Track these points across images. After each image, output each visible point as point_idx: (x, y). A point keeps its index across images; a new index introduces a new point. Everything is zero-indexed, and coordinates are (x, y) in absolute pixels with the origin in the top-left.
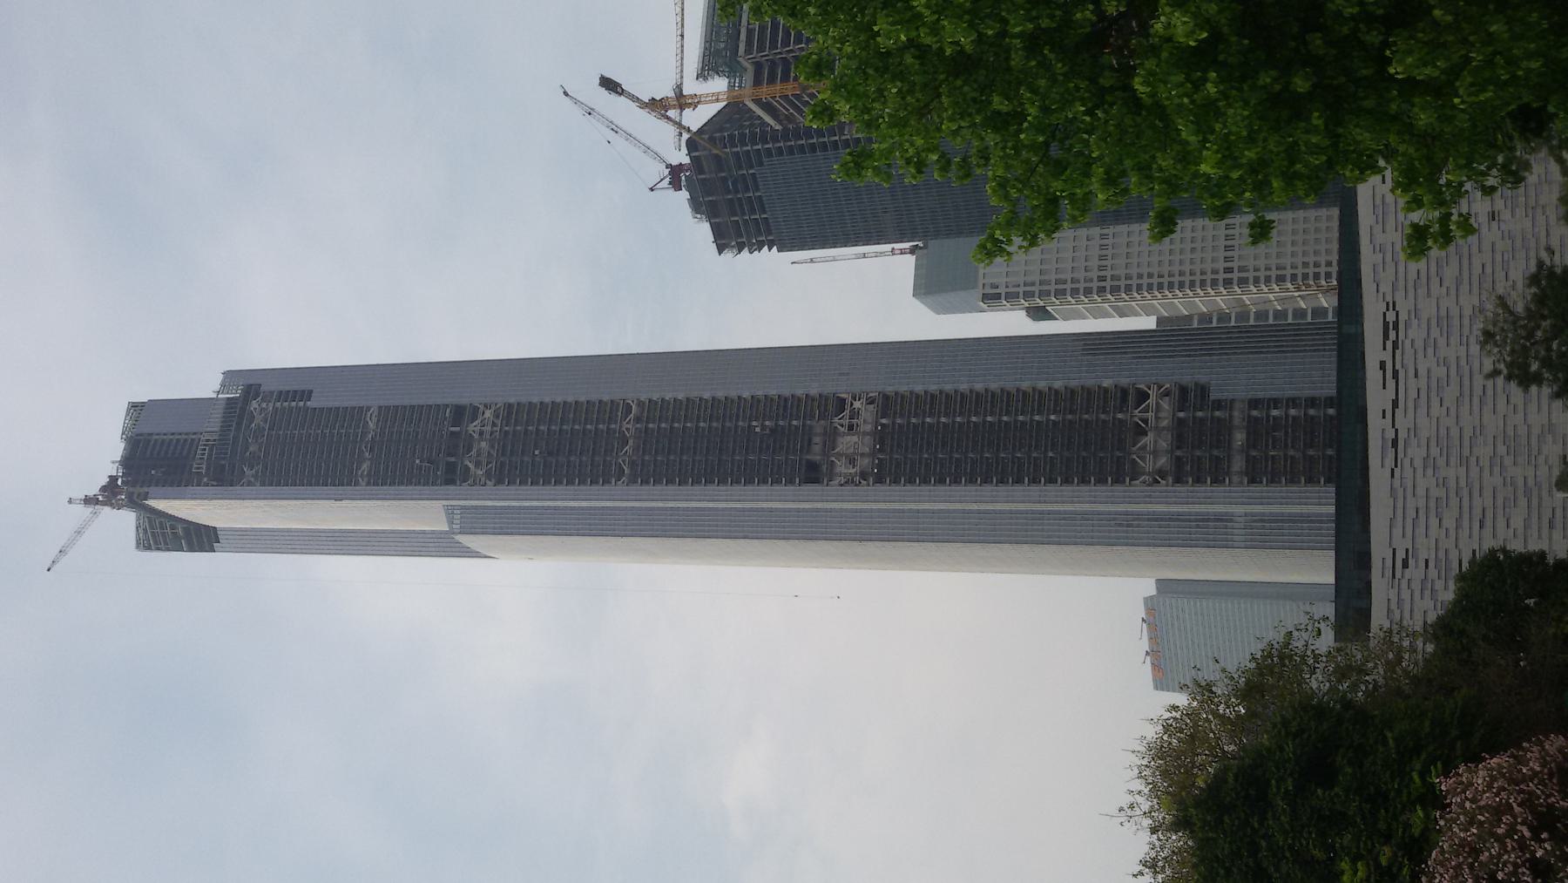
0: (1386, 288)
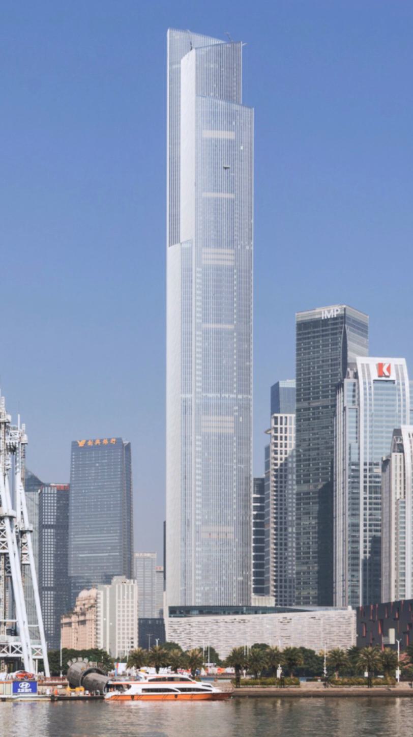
0: (253, 620)
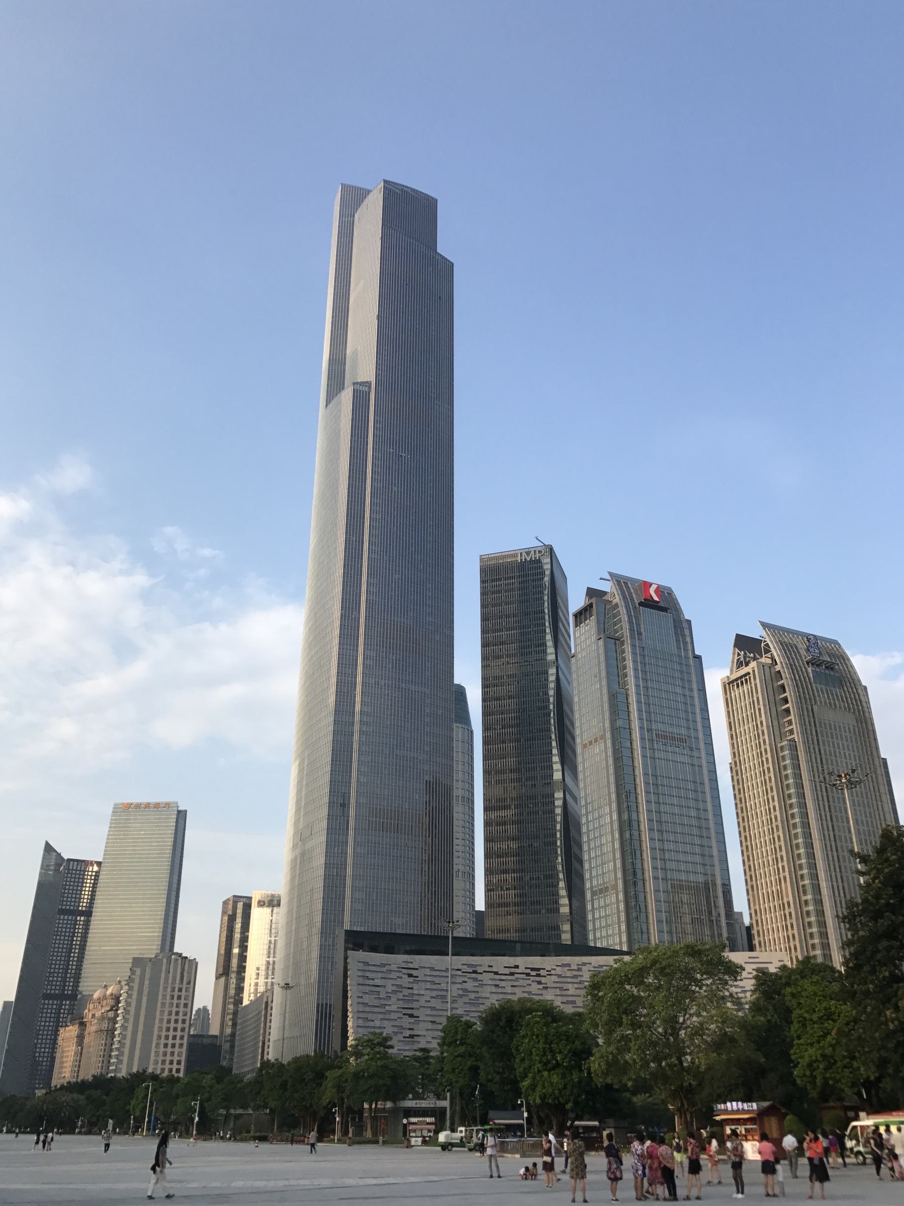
0: (559, 970)
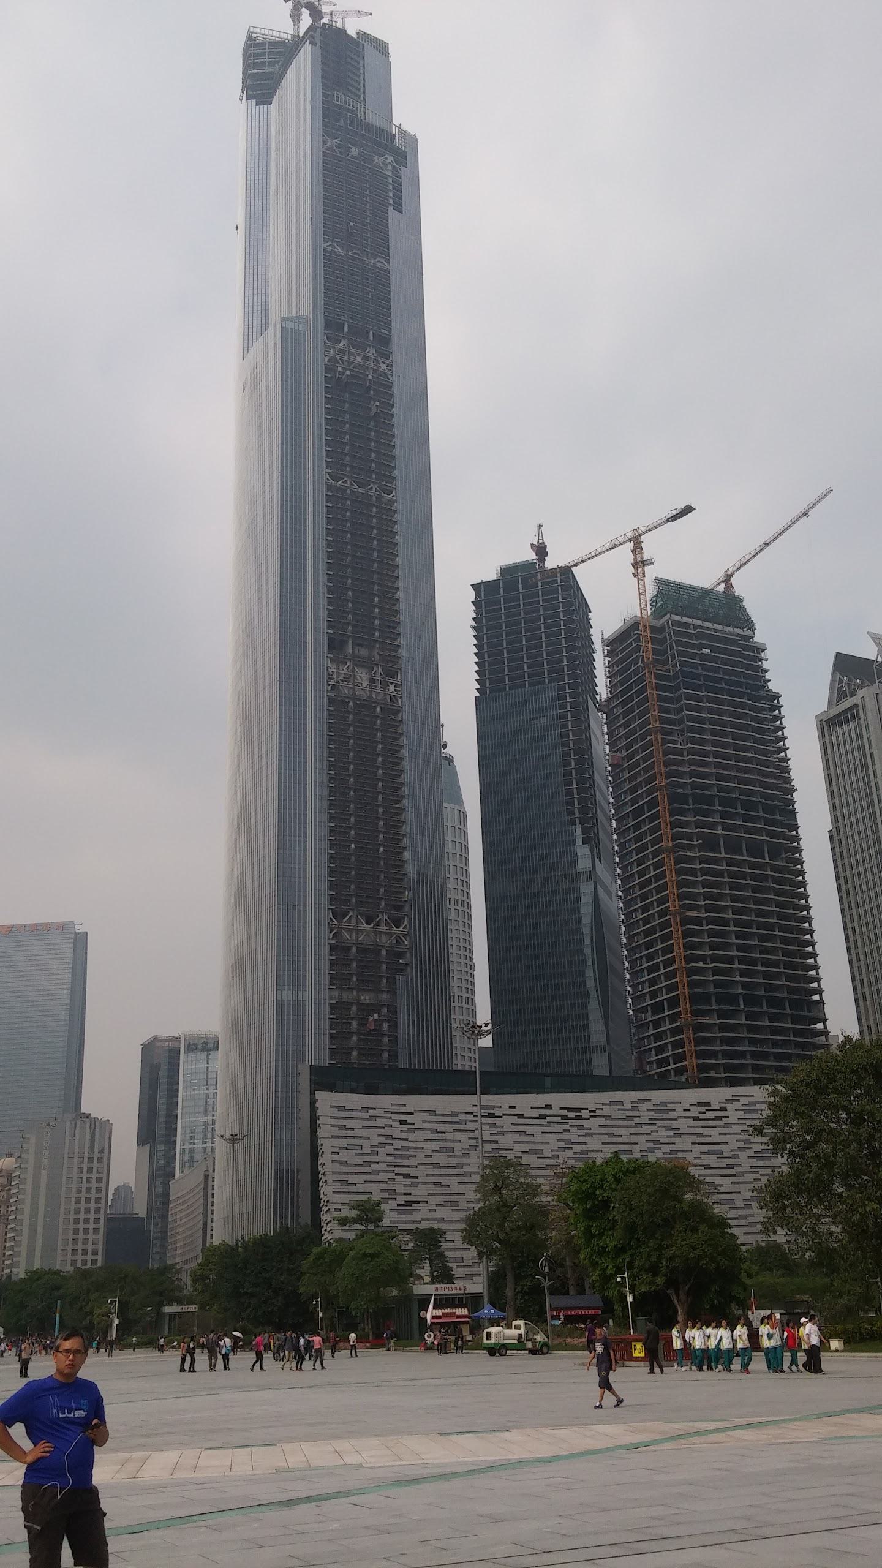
0: (607, 1111)
